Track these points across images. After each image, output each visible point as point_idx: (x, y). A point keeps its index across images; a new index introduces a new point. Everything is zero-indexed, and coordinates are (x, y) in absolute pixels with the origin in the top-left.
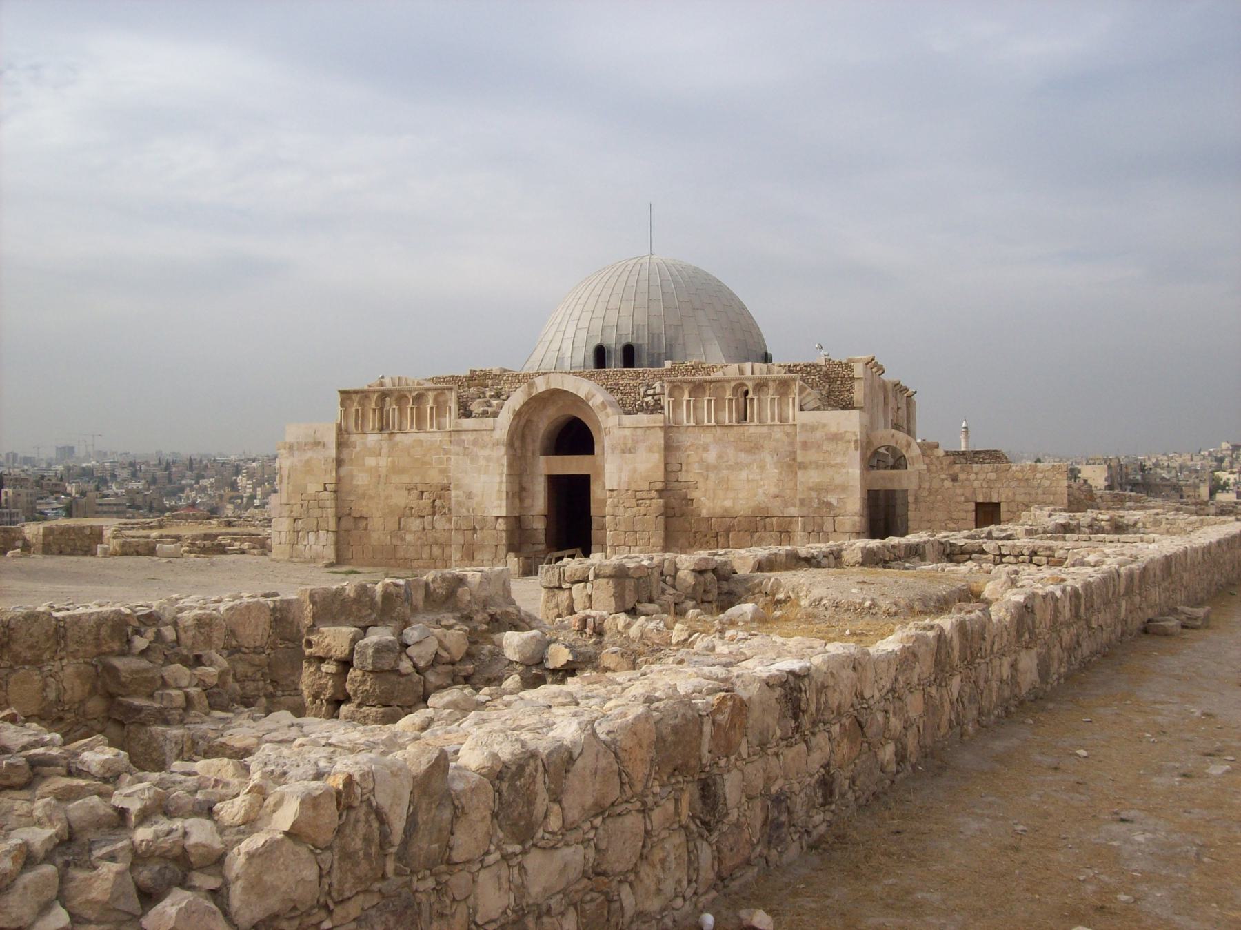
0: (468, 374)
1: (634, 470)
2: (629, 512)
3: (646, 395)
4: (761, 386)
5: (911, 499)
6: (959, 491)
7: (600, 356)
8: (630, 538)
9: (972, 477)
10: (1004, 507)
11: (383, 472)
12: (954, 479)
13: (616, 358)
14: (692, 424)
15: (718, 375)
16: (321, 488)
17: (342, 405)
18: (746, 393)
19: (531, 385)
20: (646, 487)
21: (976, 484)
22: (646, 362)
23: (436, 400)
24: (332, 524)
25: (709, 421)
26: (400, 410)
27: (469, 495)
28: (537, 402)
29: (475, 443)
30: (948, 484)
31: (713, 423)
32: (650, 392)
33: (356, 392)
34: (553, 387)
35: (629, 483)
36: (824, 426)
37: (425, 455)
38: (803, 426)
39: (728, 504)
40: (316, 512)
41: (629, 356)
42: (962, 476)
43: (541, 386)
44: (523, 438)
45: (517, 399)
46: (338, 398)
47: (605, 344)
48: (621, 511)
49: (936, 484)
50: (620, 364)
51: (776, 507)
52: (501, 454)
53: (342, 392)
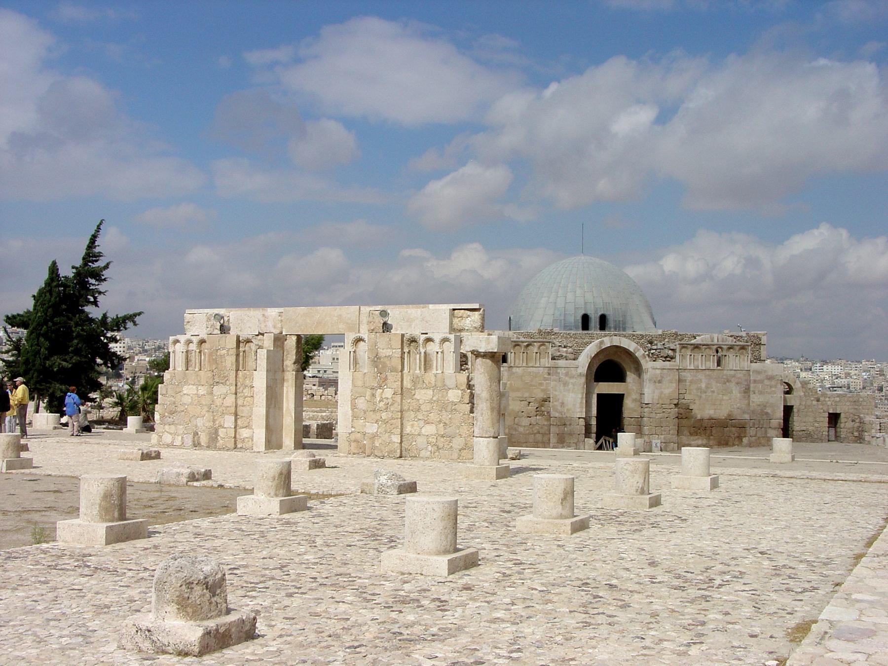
1: (661, 393)
4: (731, 348)
5: (795, 410)
8: (658, 430)
10: (842, 416)
12: (818, 400)
13: (594, 322)
20: (668, 402)
21: (829, 403)
30: (815, 403)
36: (765, 371)
37: (532, 381)
38: (754, 371)
39: (712, 412)
47: (589, 313)
48: (653, 415)
49: (809, 403)
51: (737, 414)
52: (583, 380)
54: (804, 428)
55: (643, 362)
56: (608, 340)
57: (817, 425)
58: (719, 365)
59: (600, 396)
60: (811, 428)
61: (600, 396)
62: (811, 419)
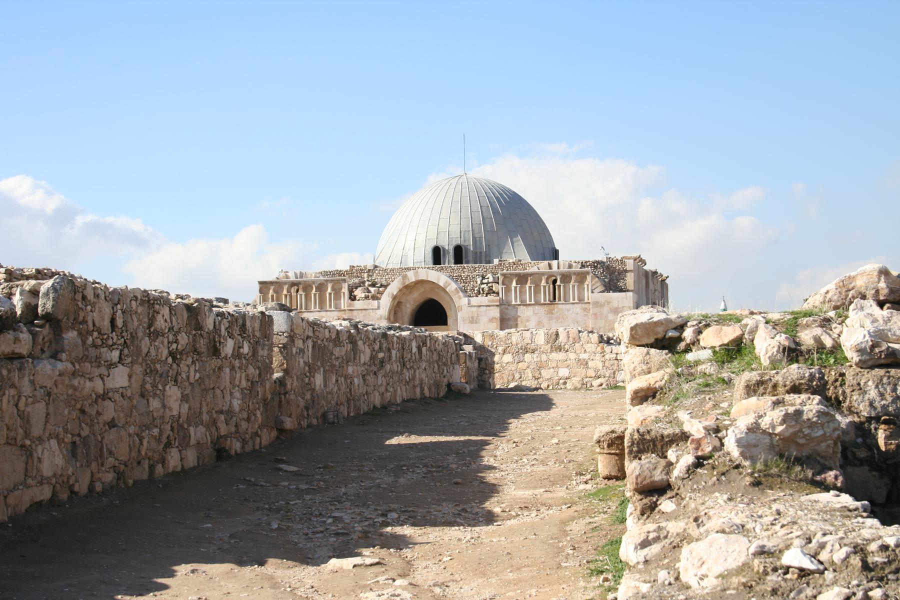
0: (348, 268)
3: (483, 284)
7: (437, 255)
14: (518, 303)
15: (534, 269)
17: (261, 292)
18: (555, 282)
19: (405, 277)
22: (471, 258)
23: (333, 289)
25: (530, 301)
26: (306, 296)
28: (408, 288)
31: (533, 302)
32: (485, 281)
33: (272, 283)
34: (420, 278)
41: (459, 254)
43: (412, 277)
44: (395, 313)
45: (394, 288)
46: (257, 287)
47: (440, 244)
50: (452, 260)
53: (260, 283)
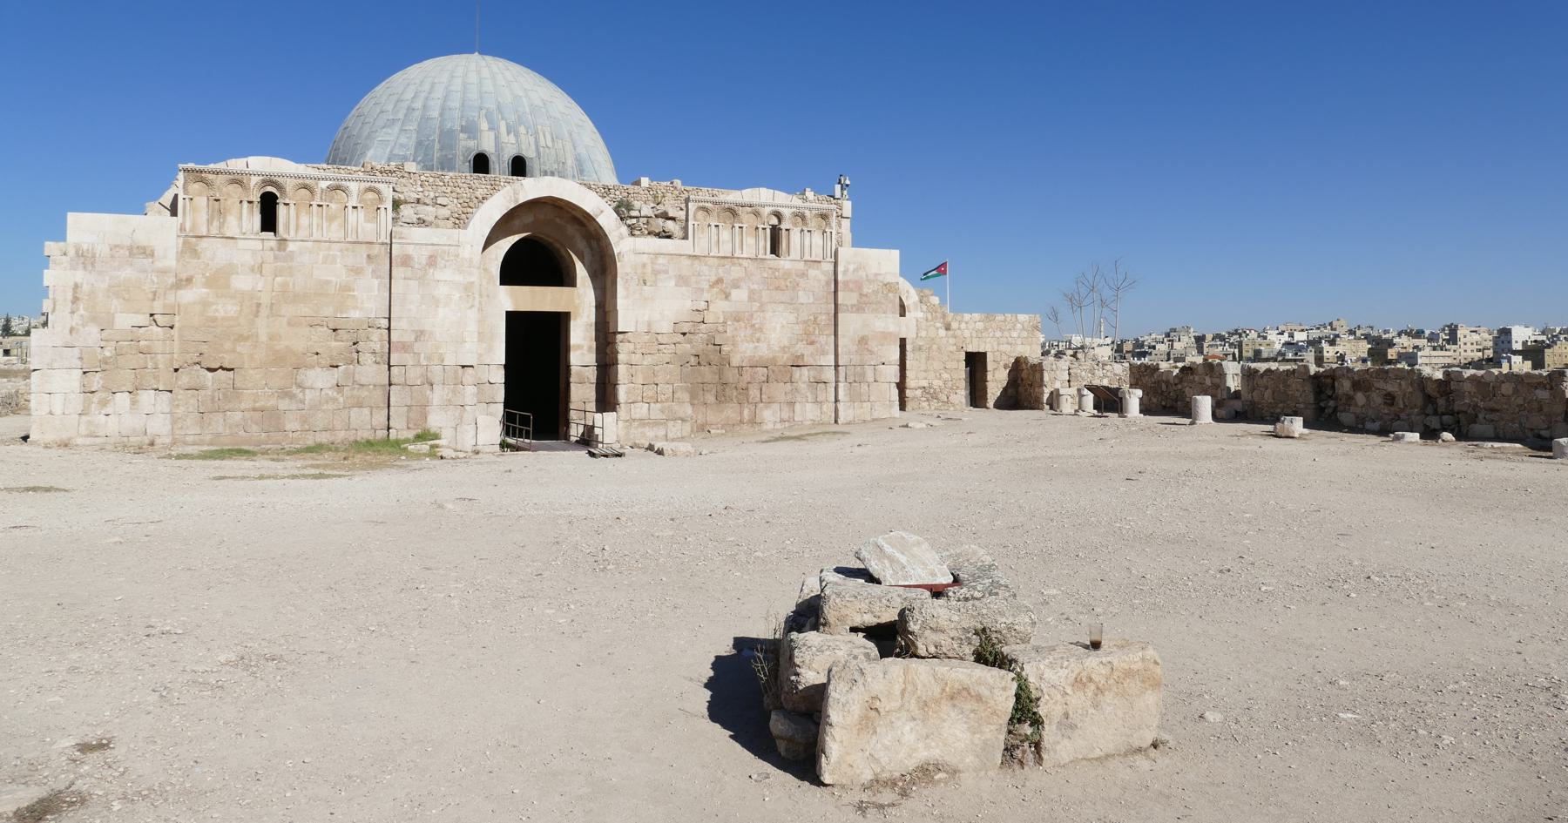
2: (648, 360)
6: (952, 341)
9: (963, 326)
11: (265, 299)
12: (948, 328)
16: (143, 319)
21: (967, 333)
24: (166, 379)
27: (420, 334)
29: (432, 261)
30: (942, 332)
35: (649, 324)
40: (135, 360)
42: (954, 325)
48: (636, 358)
54: (924, 383)
55: (613, 238)
56: (531, 188)
57: (945, 376)
58: (775, 249)
59: (513, 318)
60: (937, 383)
61: (513, 318)
62: (936, 365)
